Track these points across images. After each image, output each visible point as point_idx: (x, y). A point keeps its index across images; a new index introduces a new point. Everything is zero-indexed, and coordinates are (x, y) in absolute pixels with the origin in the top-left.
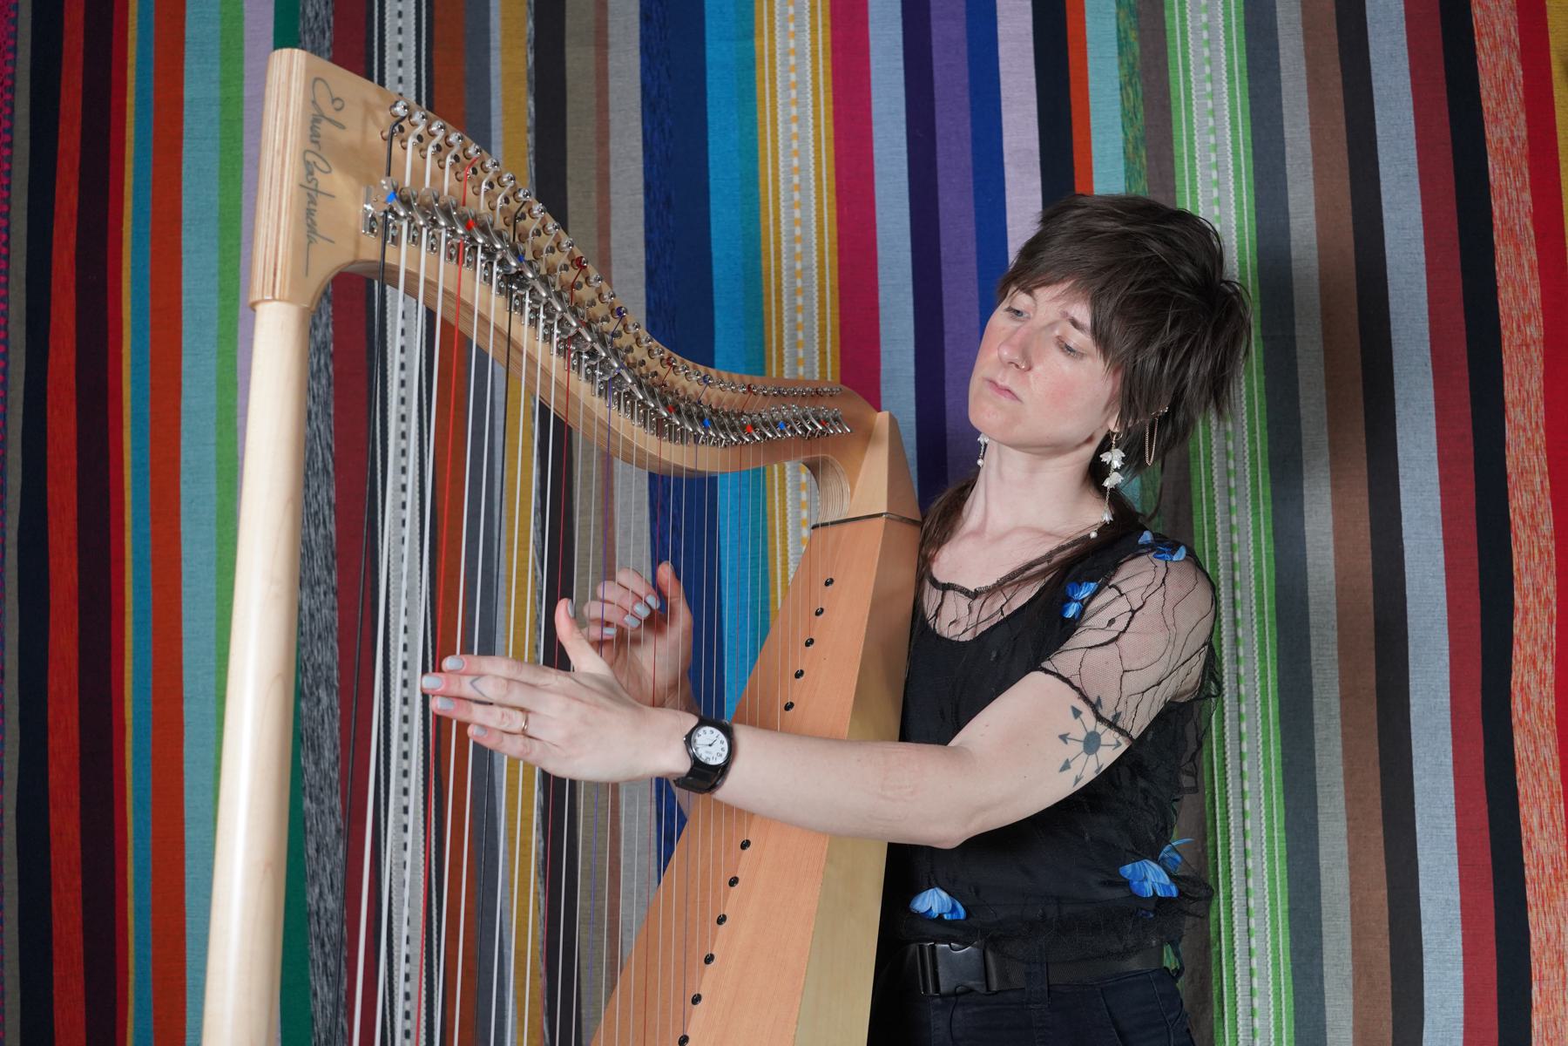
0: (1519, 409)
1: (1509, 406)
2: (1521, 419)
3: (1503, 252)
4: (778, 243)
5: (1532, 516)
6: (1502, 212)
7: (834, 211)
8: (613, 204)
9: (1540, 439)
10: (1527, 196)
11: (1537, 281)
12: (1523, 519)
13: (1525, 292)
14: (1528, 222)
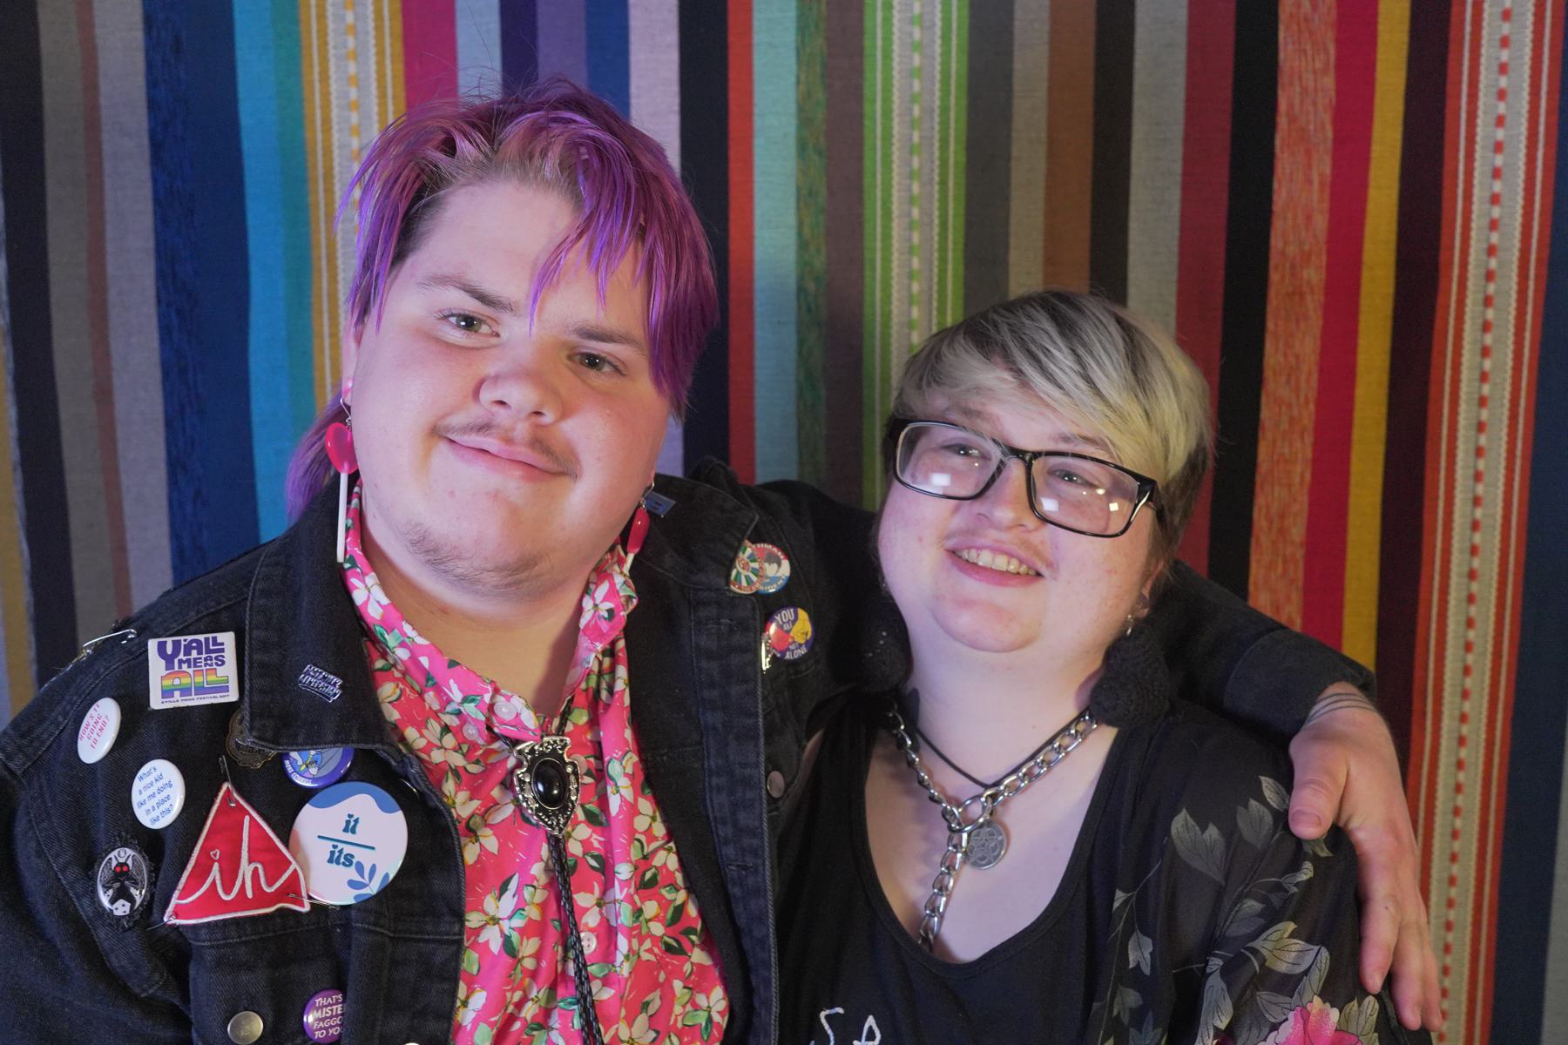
0: (1284, 379)
1: (1268, 374)
2: (1285, 393)
3: (1286, 164)
4: (326, 106)
5: (1282, 516)
6: (1291, 106)
7: (400, 66)
8: (99, 42)
9: (1308, 416)
10: (1329, 82)
11: (1326, 205)
12: (1271, 521)
13: (1309, 218)
14: (1327, 118)
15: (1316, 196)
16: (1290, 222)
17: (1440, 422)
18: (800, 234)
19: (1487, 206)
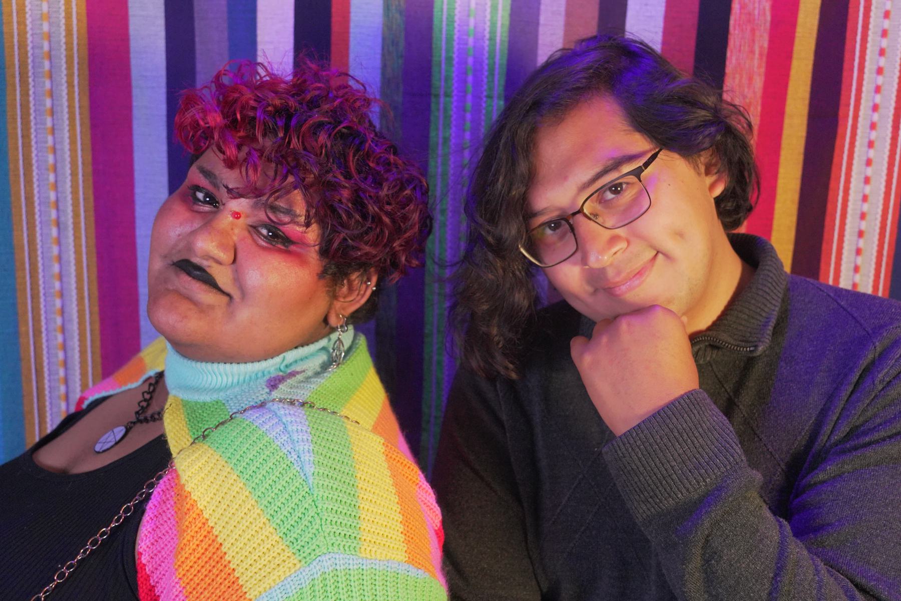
11: (763, 70)
13: (750, 79)
15: (756, 62)
16: (737, 81)
17: (833, 230)
18: (383, 74)
19: (875, 75)
